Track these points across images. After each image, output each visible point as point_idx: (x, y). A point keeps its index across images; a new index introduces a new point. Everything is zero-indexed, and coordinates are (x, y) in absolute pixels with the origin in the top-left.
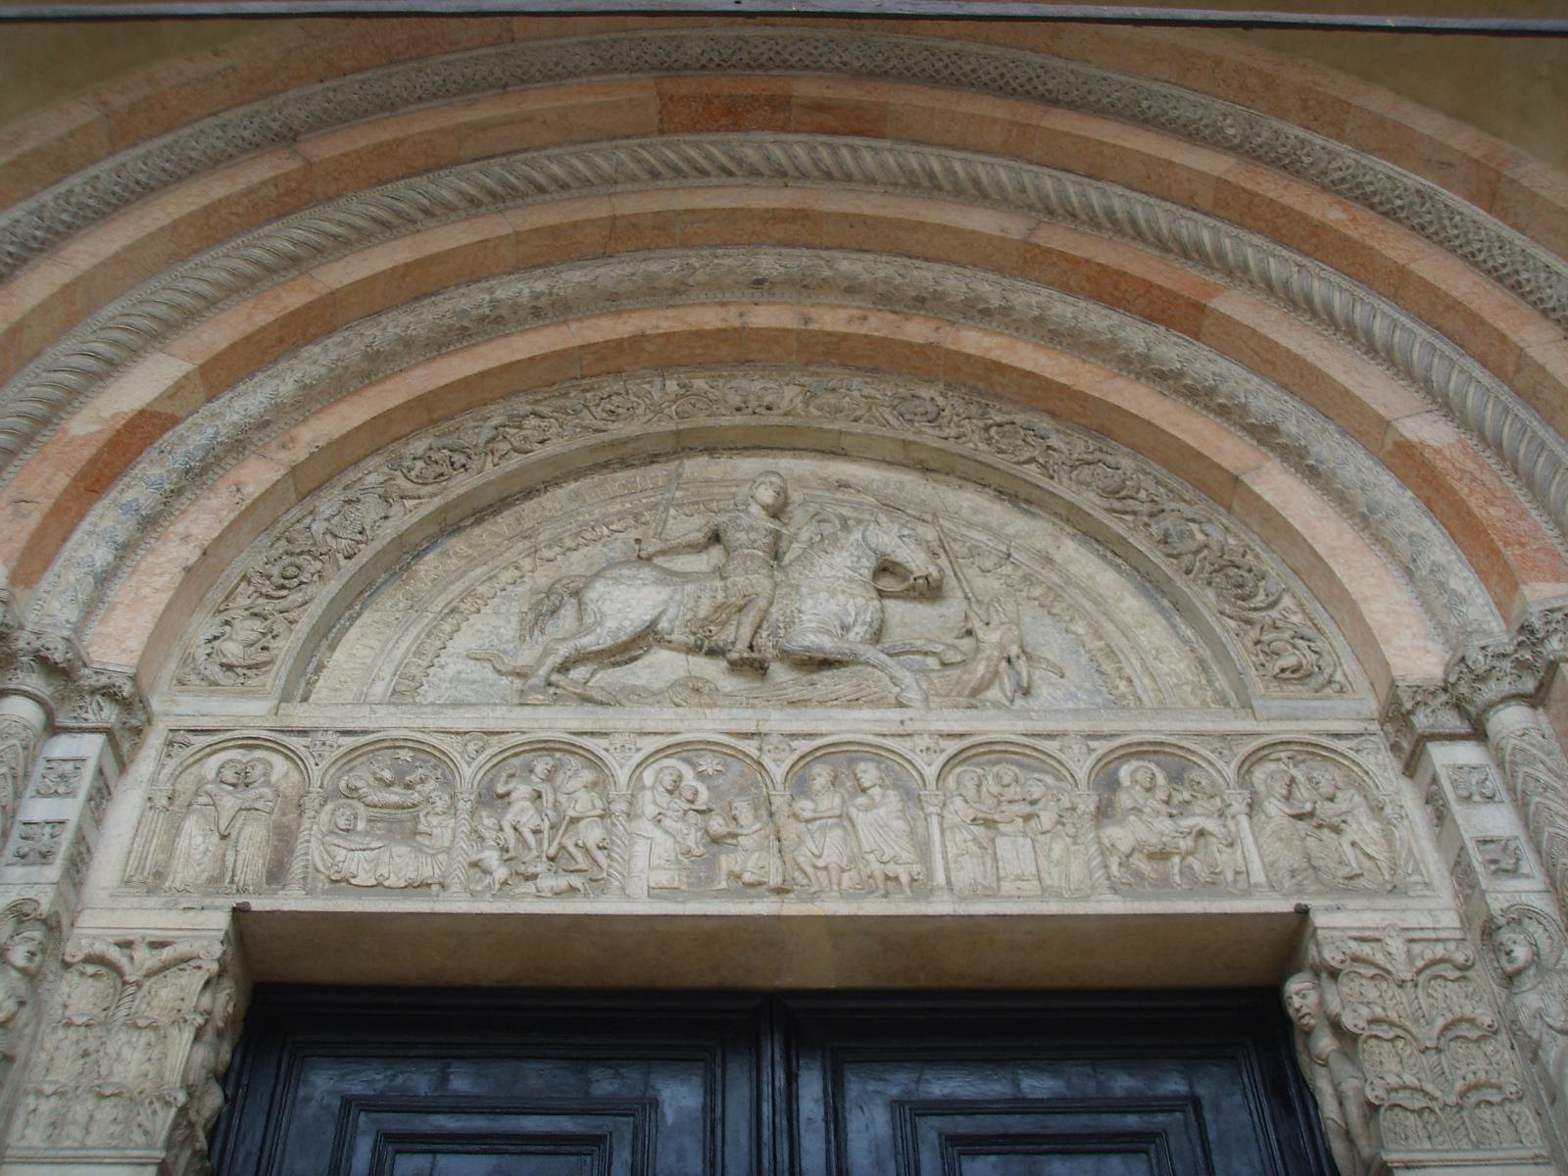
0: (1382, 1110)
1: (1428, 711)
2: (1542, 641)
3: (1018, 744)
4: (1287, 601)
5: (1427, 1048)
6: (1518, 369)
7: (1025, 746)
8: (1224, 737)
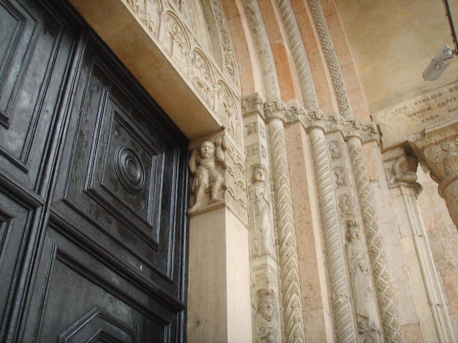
0: (227, 190)
1: (260, 107)
2: (298, 114)
3: (182, 24)
4: (230, 52)
5: (236, 183)
6: (314, 54)
7: (183, 27)
8: (217, 71)
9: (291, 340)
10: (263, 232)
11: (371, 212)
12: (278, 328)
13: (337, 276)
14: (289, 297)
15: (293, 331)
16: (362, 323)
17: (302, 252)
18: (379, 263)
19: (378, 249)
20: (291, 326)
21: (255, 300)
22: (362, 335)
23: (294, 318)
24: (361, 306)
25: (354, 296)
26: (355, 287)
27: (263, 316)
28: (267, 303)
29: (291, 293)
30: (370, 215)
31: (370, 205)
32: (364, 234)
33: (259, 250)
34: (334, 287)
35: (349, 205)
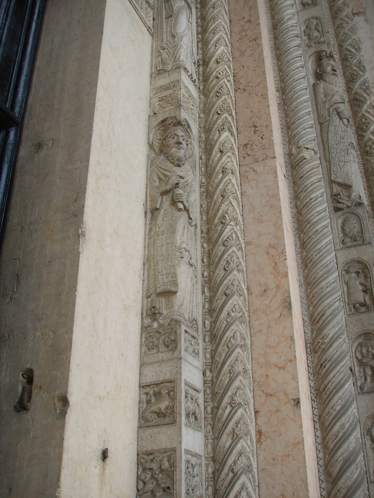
9: (216, 202)
10: (176, 38)
11: (354, 47)
12: (193, 183)
13: (300, 121)
14: (216, 138)
15: (221, 187)
16: (339, 194)
17: (242, 81)
18: (367, 115)
19: (365, 95)
20: (216, 181)
21: (155, 136)
22: (340, 213)
23: (223, 168)
24: (339, 169)
25: (327, 155)
26: (329, 141)
27: (167, 157)
28: (176, 137)
29: (221, 130)
30: (353, 51)
31: (354, 38)
32: (342, 78)
33: (169, 64)
34: (295, 136)
35: (320, 30)
